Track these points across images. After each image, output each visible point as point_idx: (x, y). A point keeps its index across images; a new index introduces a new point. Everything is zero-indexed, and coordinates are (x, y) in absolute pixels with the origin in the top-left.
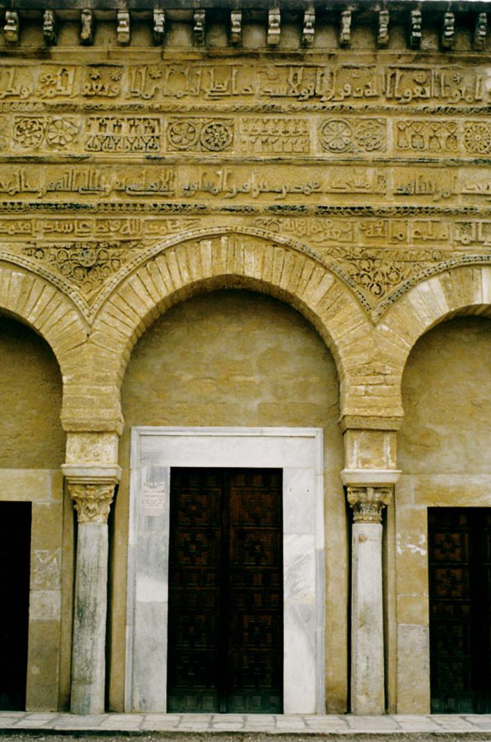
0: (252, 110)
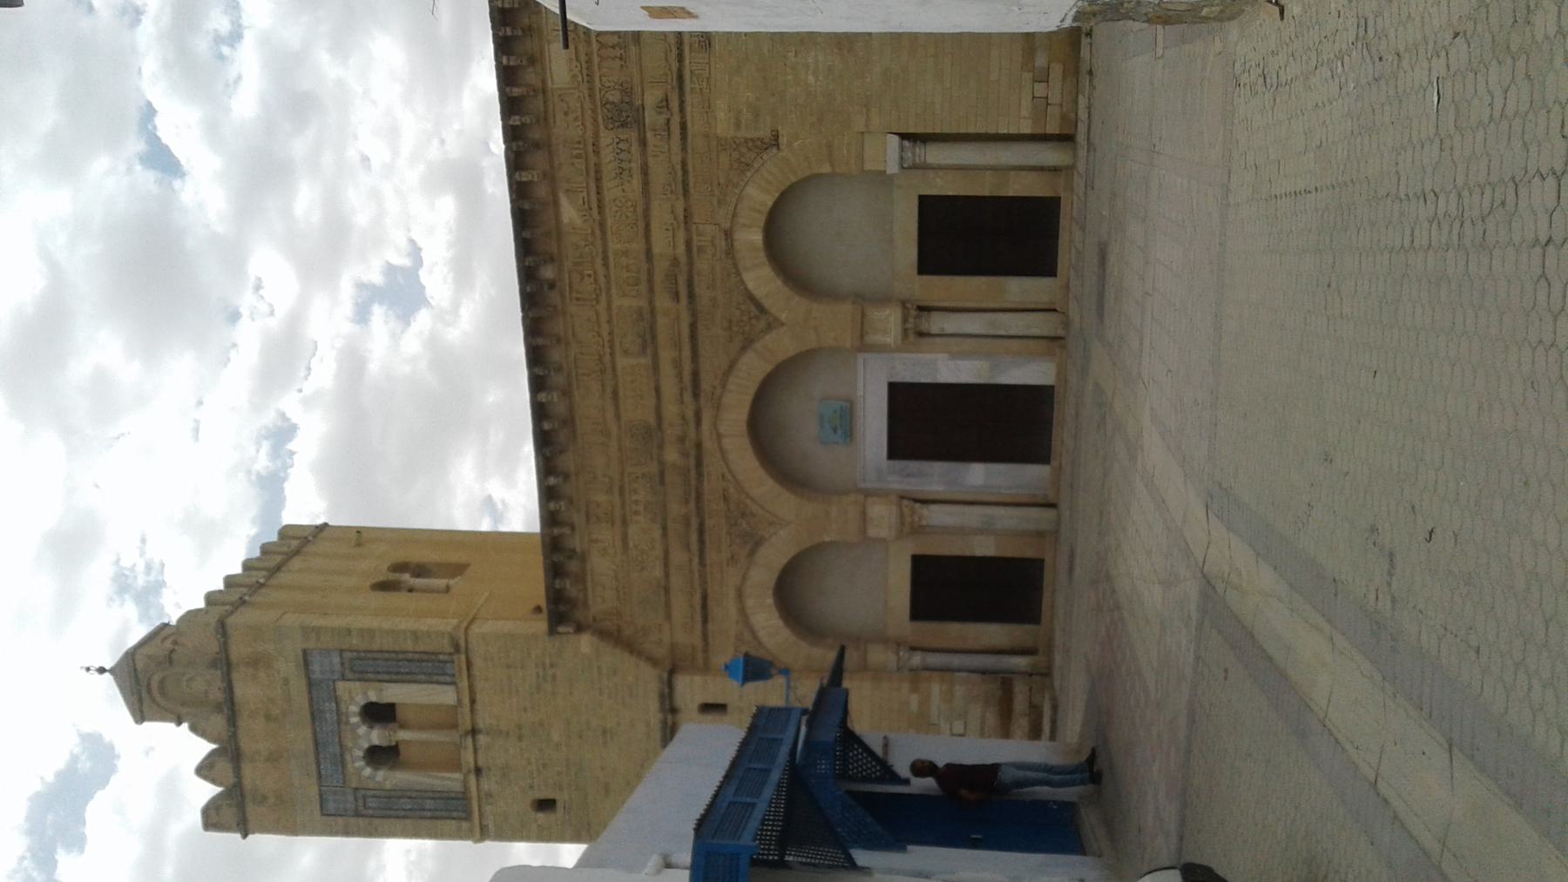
0: (617, 407)
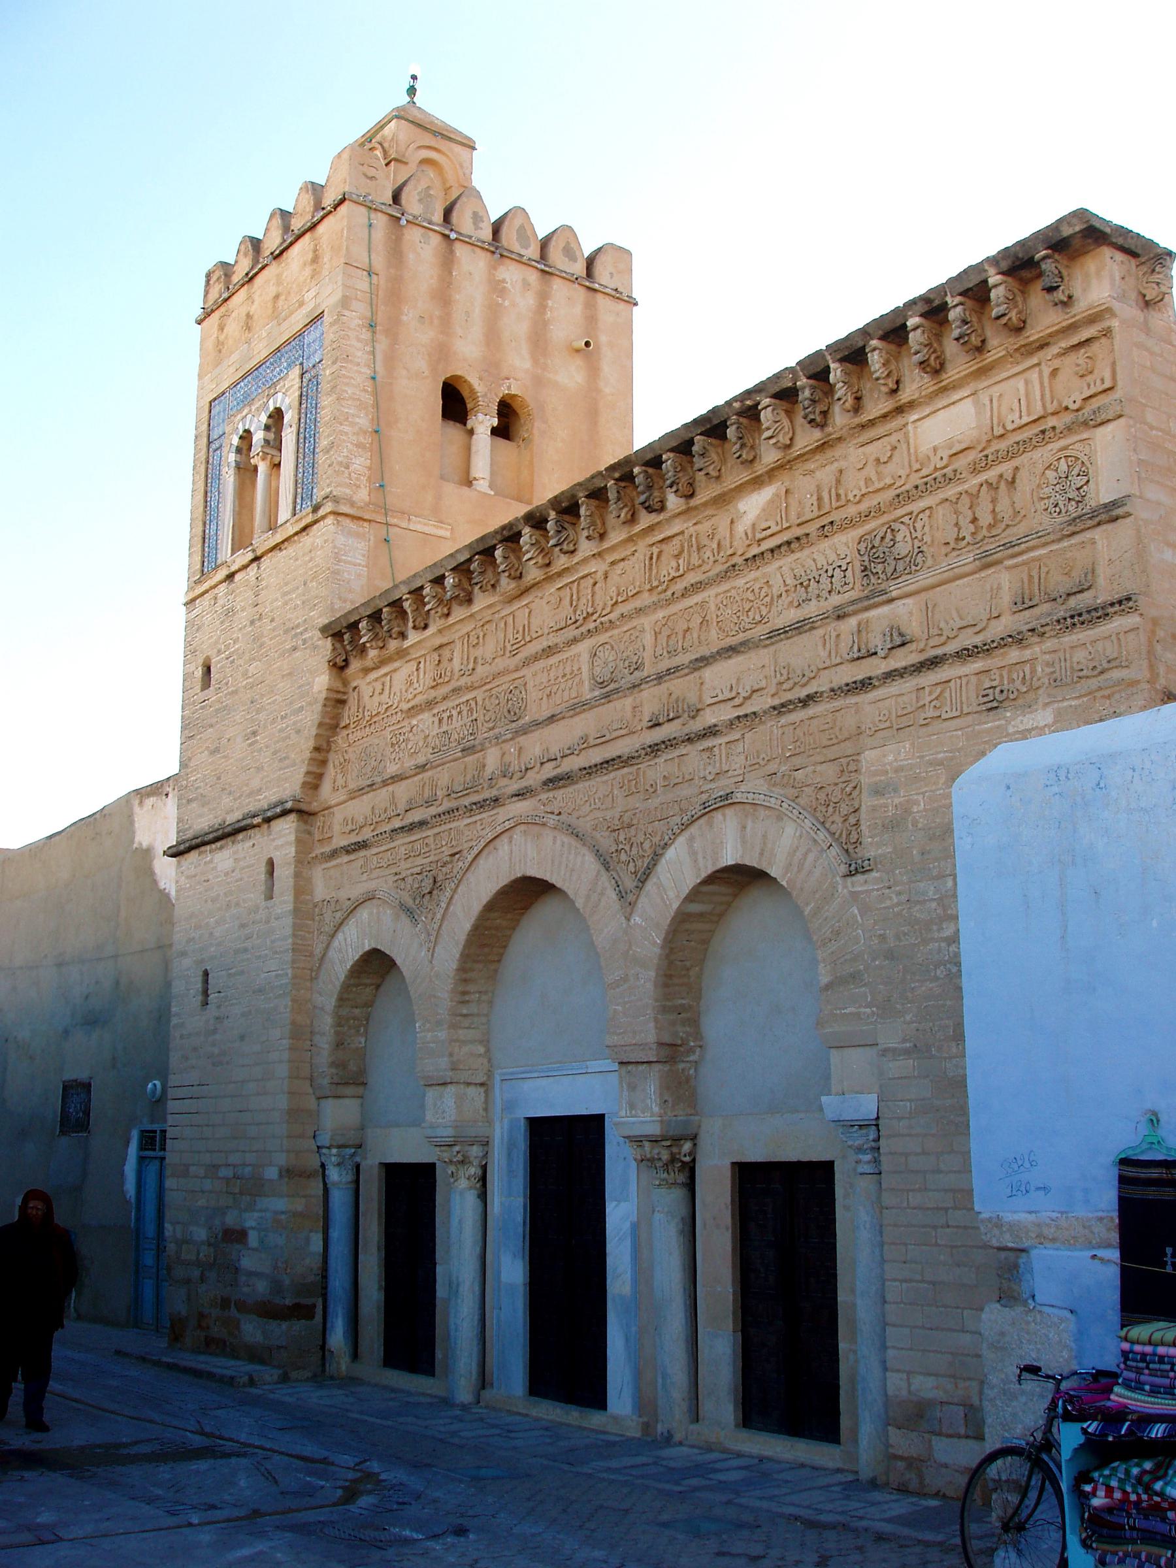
0: (536, 658)
